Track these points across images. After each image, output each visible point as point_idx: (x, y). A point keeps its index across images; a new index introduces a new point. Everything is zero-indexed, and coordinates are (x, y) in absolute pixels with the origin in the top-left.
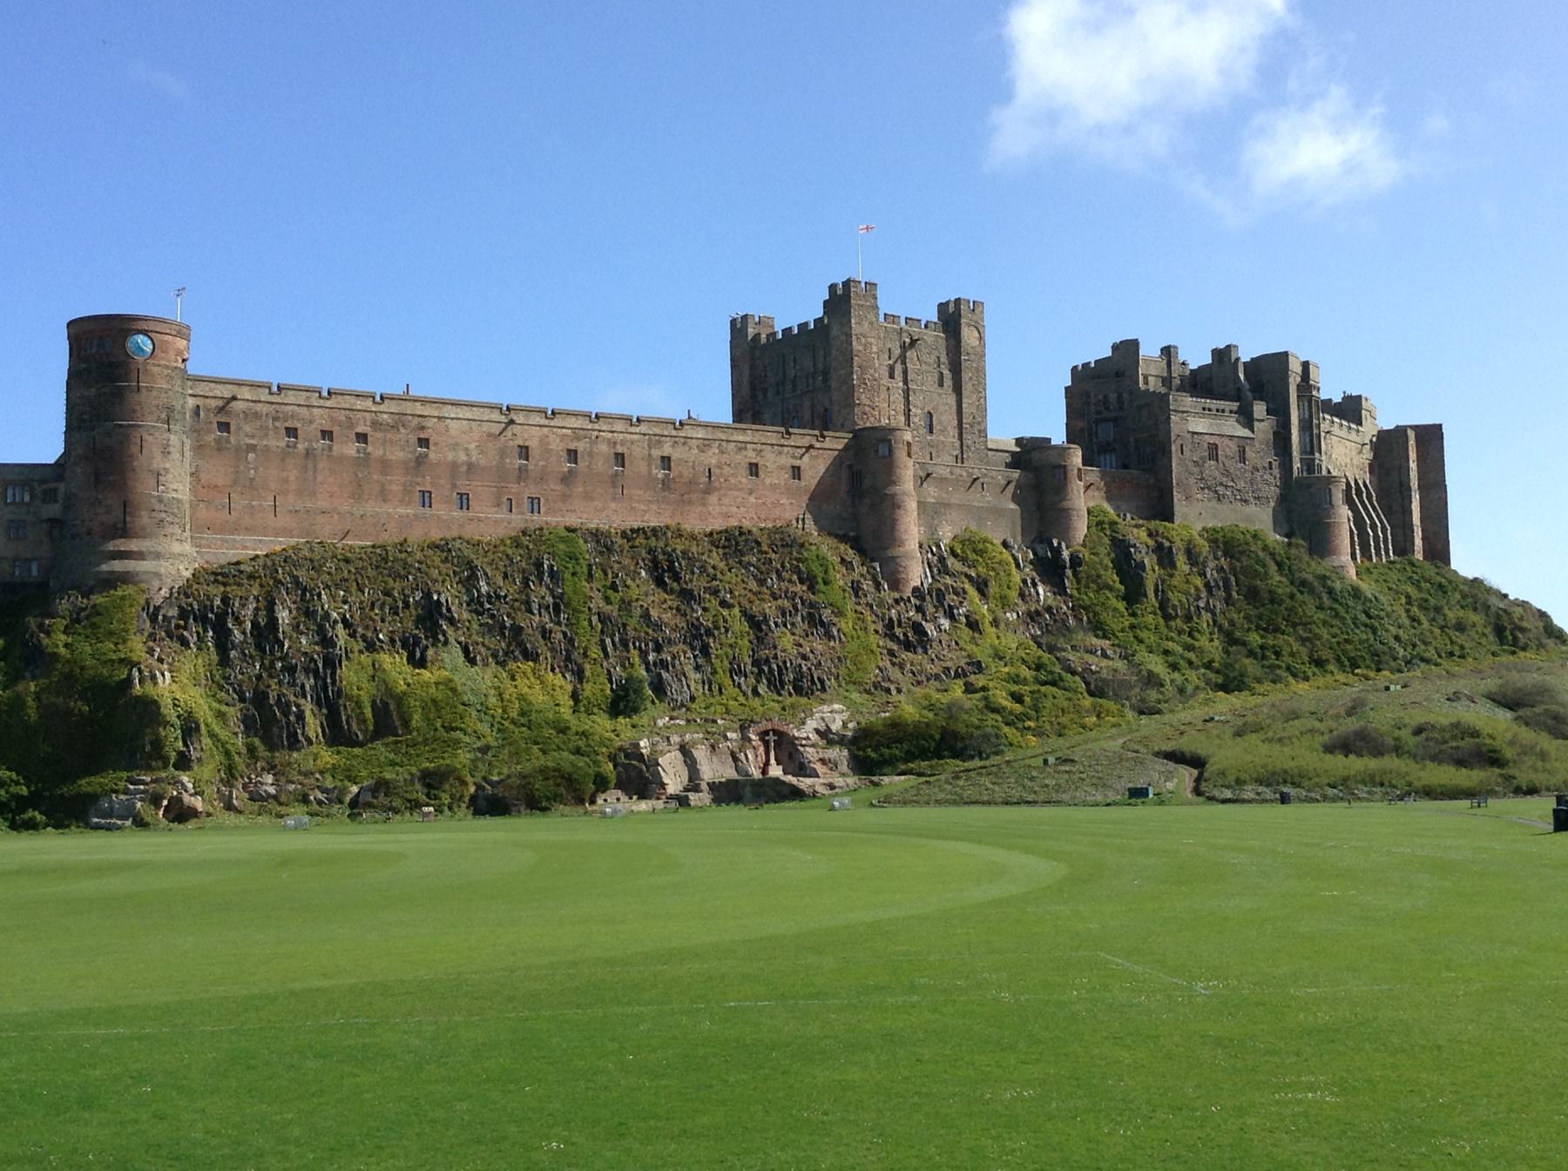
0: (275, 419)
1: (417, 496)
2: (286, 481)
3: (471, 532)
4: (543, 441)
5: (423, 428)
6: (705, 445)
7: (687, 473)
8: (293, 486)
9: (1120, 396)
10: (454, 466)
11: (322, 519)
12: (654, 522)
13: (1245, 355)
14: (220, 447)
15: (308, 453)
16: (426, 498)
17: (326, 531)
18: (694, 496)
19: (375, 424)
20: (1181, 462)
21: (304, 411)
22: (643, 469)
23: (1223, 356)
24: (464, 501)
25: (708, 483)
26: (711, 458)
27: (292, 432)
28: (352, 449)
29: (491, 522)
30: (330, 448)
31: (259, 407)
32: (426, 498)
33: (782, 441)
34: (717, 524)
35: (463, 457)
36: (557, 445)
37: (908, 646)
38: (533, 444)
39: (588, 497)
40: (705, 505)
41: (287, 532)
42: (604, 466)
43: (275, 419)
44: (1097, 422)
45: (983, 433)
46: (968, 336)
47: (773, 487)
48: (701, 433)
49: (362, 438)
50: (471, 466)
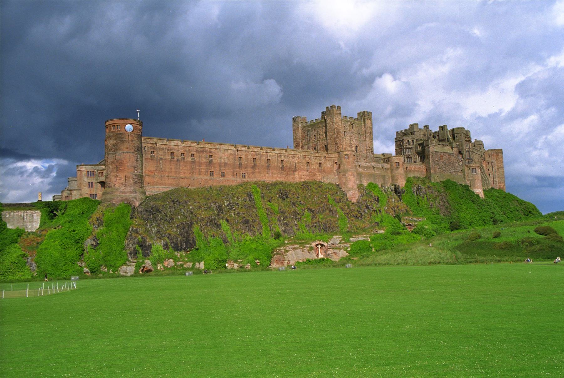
0: (168, 150)
1: (209, 173)
2: (171, 169)
3: (226, 184)
4: (247, 157)
5: (211, 152)
8: (173, 170)
9: (413, 141)
10: (220, 164)
11: (182, 180)
12: (279, 180)
13: (449, 128)
14: (152, 158)
15: (178, 160)
16: (212, 174)
17: (184, 183)
18: (291, 172)
20: (433, 160)
21: (176, 147)
22: (276, 164)
23: (443, 128)
24: (223, 175)
28: (190, 159)
30: (184, 158)
31: (163, 146)
32: (212, 174)
33: (317, 155)
35: (223, 161)
36: (250, 157)
37: (357, 217)
38: (243, 156)
39: (259, 173)
40: (294, 175)
41: (171, 184)
42: (264, 163)
43: (168, 150)
44: (406, 149)
45: (372, 152)
46: (368, 122)
47: (314, 169)
49: (193, 155)
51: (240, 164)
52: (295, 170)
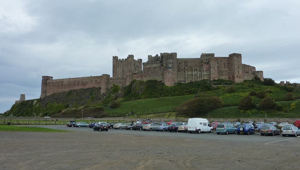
6: (87, 79)
7: (85, 82)
17: (55, 92)
19: (59, 82)
24: (65, 88)
25: (87, 83)
26: (87, 81)
27: (53, 84)
29: (67, 90)
34: (87, 88)
36: (73, 81)
38: (71, 82)
50: (66, 85)
51: (70, 84)
52: (87, 84)
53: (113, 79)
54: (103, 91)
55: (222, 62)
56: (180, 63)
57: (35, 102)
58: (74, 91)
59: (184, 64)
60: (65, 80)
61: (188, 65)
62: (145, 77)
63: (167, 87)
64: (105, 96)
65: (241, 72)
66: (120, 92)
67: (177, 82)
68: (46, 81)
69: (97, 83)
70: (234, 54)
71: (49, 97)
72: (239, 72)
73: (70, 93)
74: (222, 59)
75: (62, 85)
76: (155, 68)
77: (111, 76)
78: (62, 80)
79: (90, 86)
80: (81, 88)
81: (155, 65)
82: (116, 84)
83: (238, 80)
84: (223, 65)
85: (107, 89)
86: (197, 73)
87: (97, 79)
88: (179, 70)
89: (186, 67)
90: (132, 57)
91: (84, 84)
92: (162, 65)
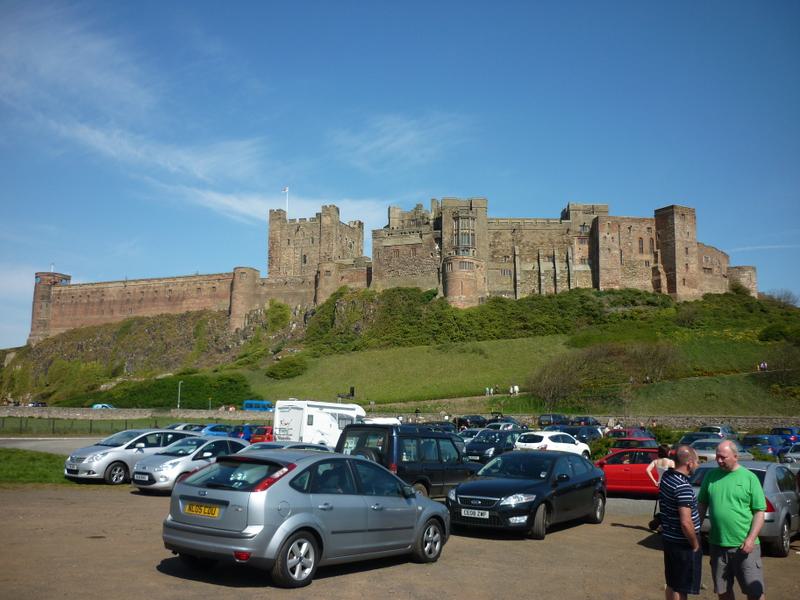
4: (134, 292)
10: (110, 302)
17: (78, 325)
19: (92, 292)
26: (185, 288)
29: (119, 317)
34: (183, 311)
48: (181, 280)
52: (183, 299)
53: (271, 284)
54: (238, 323)
55: (632, 234)
56: (497, 234)
57: (12, 356)
58: (141, 321)
59: (510, 237)
60: (110, 285)
61: (524, 241)
62: (381, 276)
63: (456, 309)
64: (245, 338)
65: (693, 267)
66: (294, 325)
67: (488, 294)
68: (50, 287)
69: (217, 296)
70: (672, 207)
71: (55, 341)
72: (690, 266)
73: (126, 328)
74: (634, 225)
75: (102, 301)
76: (414, 247)
77: (264, 274)
78: (102, 286)
79: (192, 305)
80: (165, 312)
81: (414, 239)
82: (280, 301)
83: (684, 293)
84: (636, 244)
85: (251, 317)
86: (554, 267)
87: (217, 284)
88: (492, 257)
89: (517, 247)
90: (335, 213)
91: (173, 300)
92: (439, 240)
